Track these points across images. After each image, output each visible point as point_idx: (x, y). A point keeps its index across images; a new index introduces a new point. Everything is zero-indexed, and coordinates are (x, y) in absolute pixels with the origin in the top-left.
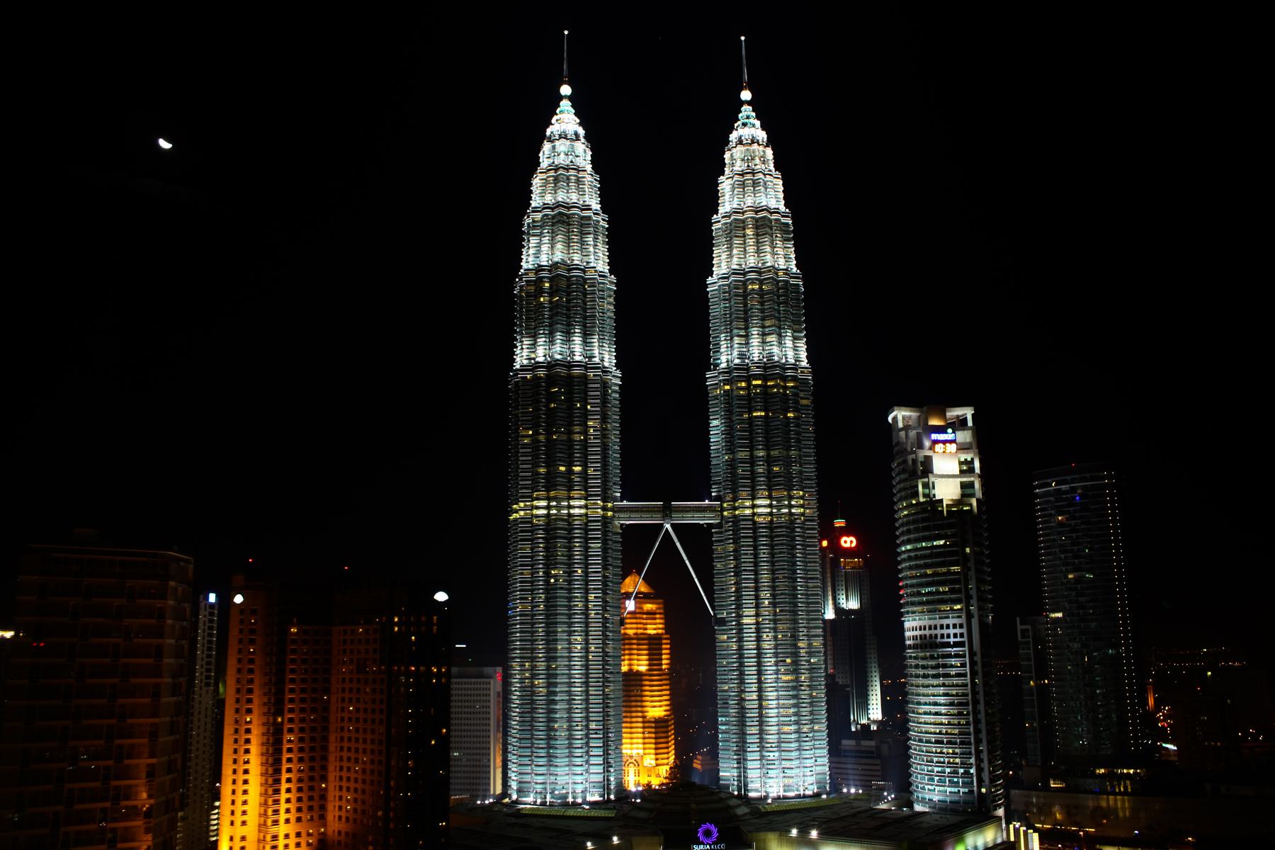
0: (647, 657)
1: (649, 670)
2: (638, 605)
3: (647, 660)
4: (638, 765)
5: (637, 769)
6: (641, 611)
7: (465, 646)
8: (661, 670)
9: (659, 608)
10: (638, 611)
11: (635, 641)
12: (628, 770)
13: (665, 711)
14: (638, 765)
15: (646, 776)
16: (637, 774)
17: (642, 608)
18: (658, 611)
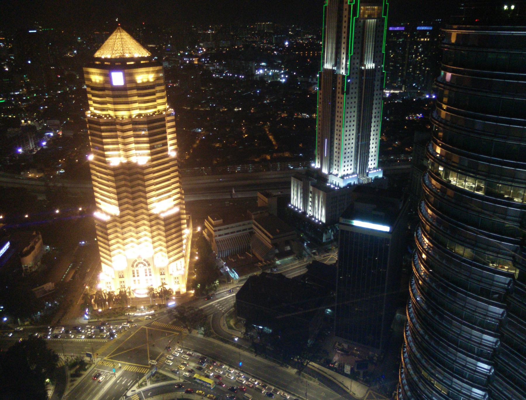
0: (148, 145)
1: (153, 160)
2: (128, 78)
3: (147, 149)
4: (149, 265)
5: (147, 268)
6: (134, 85)
7: (30, 31)
8: (167, 156)
9: (157, 79)
10: (128, 86)
11: (130, 126)
12: (137, 271)
13: (175, 200)
14: (149, 265)
15: (159, 274)
16: (148, 274)
17: (134, 81)
18: (157, 82)
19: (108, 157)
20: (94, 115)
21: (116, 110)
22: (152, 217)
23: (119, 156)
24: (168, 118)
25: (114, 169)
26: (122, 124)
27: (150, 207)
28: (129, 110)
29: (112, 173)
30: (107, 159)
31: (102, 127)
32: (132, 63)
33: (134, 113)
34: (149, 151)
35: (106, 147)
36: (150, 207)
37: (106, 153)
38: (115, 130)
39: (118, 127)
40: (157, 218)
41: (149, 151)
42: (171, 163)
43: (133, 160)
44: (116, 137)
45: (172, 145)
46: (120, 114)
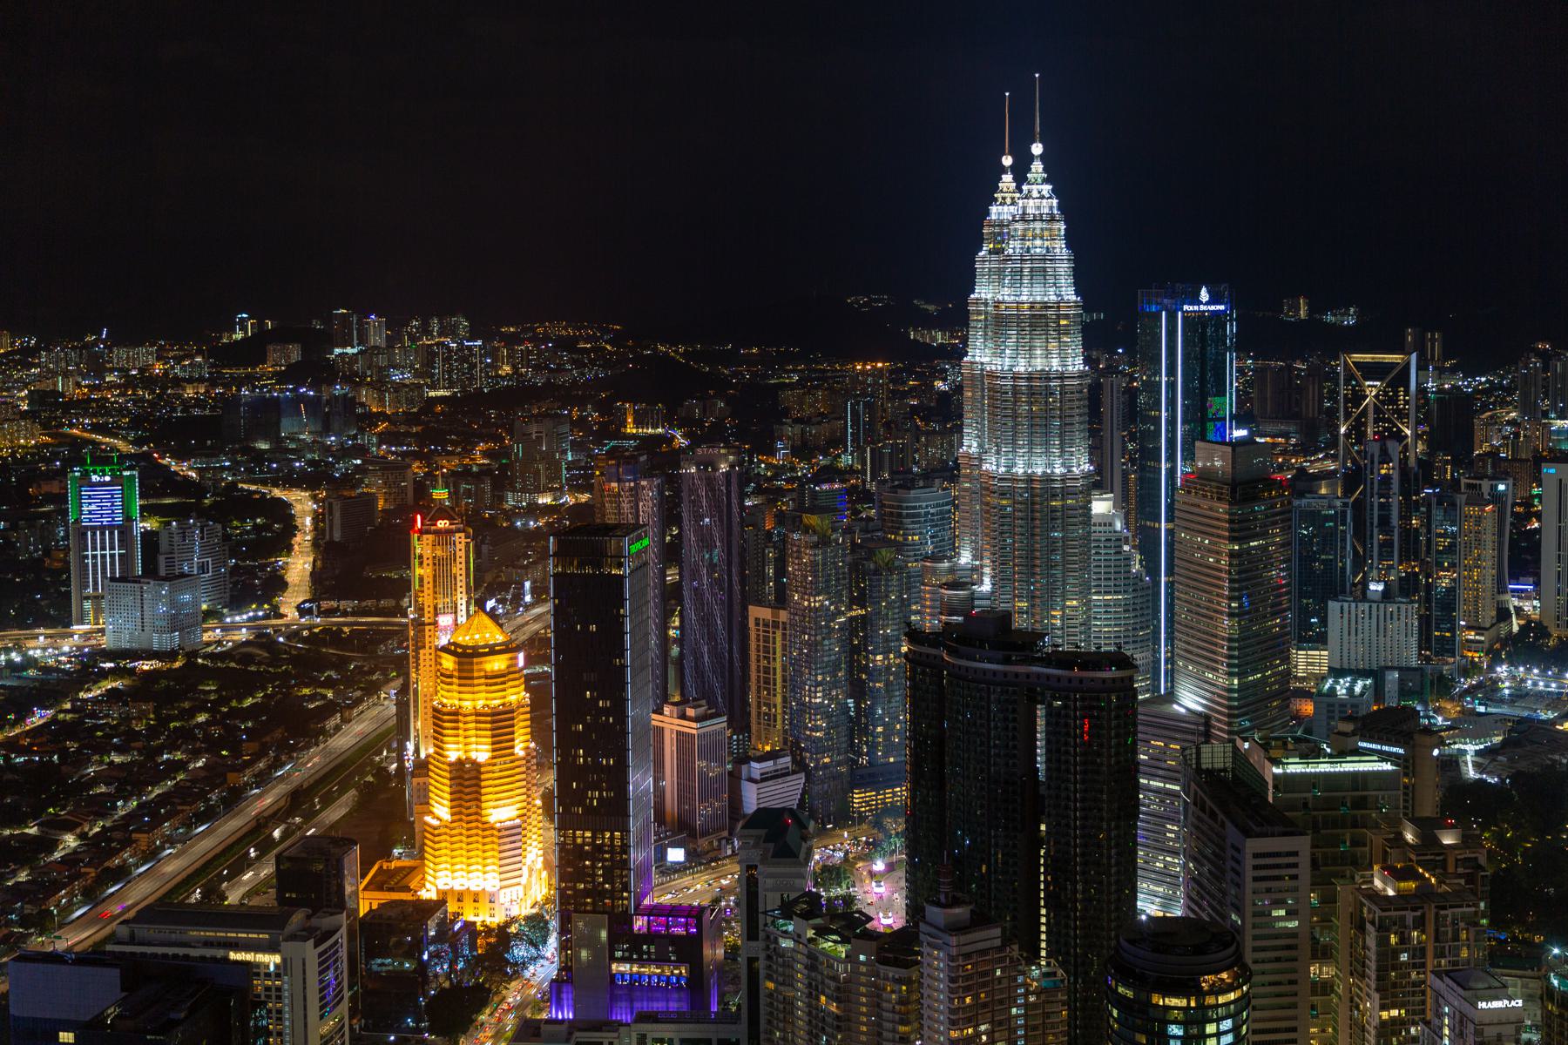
1: (494, 758)
6: (482, 674)
8: (513, 754)
11: (473, 718)
19: (447, 750)
20: (441, 703)
21: (460, 700)
22: (486, 826)
23: (458, 750)
24: (522, 710)
25: (450, 764)
26: (465, 716)
27: (483, 812)
28: (473, 700)
29: (448, 768)
30: (446, 753)
31: (445, 717)
32: (487, 650)
33: (479, 704)
34: (489, 747)
35: (445, 739)
36: (483, 812)
37: (445, 746)
38: (457, 721)
39: (461, 718)
40: (493, 828)
41: (489, 747)
42: (516, 763)
43: (473, 755)
44: (457, 728)
45: (522, 738)
46: (464, 704)
